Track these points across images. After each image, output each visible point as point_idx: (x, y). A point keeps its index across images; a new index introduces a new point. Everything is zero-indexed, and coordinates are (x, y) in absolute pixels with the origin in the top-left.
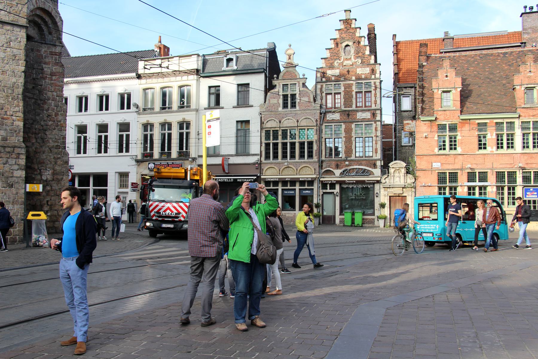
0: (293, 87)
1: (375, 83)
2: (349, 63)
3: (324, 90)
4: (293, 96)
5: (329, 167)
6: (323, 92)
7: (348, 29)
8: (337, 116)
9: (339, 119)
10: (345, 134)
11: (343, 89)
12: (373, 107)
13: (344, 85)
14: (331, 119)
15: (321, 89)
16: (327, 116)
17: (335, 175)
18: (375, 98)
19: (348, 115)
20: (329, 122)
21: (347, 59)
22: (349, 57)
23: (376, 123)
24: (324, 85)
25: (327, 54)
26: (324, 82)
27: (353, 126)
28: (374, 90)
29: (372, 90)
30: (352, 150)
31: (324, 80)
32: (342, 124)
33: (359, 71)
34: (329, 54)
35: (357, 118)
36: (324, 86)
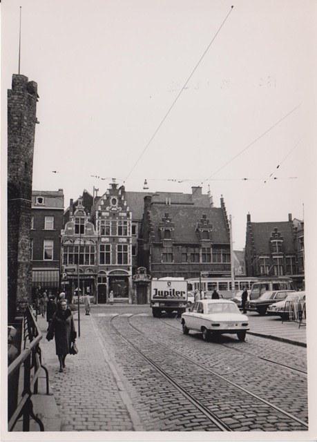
2: (115, 209)
4: (82, 227)
12: (128, 236)
13: (112, 222)
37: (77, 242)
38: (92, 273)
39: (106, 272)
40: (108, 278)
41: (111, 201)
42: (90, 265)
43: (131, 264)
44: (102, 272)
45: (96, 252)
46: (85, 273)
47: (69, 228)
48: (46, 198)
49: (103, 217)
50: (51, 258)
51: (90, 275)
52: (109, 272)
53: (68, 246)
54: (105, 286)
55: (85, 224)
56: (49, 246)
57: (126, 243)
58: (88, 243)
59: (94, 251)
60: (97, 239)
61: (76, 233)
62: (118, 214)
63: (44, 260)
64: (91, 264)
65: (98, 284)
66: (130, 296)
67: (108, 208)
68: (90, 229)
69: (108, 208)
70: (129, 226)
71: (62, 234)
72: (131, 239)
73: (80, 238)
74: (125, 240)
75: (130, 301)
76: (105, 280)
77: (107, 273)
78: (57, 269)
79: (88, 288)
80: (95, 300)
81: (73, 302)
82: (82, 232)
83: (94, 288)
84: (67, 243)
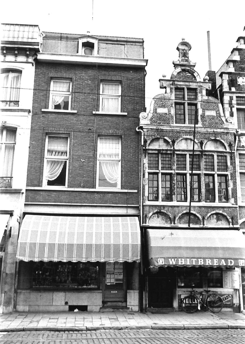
3: (234, 102)
6: (234, 107)
24: (234, 96)
26: (233, 93)
31: (233, 89)
42: (217, 204)
48: (103, 45)
50: (115, 185)
58: (209, 146)
60: (231, 138)
63: (98, 189)
64: (220, 201)
68: (213, 113)
71: (143, 122)
78: (131, 211)
81: (176, 304)
84: (156, 146)
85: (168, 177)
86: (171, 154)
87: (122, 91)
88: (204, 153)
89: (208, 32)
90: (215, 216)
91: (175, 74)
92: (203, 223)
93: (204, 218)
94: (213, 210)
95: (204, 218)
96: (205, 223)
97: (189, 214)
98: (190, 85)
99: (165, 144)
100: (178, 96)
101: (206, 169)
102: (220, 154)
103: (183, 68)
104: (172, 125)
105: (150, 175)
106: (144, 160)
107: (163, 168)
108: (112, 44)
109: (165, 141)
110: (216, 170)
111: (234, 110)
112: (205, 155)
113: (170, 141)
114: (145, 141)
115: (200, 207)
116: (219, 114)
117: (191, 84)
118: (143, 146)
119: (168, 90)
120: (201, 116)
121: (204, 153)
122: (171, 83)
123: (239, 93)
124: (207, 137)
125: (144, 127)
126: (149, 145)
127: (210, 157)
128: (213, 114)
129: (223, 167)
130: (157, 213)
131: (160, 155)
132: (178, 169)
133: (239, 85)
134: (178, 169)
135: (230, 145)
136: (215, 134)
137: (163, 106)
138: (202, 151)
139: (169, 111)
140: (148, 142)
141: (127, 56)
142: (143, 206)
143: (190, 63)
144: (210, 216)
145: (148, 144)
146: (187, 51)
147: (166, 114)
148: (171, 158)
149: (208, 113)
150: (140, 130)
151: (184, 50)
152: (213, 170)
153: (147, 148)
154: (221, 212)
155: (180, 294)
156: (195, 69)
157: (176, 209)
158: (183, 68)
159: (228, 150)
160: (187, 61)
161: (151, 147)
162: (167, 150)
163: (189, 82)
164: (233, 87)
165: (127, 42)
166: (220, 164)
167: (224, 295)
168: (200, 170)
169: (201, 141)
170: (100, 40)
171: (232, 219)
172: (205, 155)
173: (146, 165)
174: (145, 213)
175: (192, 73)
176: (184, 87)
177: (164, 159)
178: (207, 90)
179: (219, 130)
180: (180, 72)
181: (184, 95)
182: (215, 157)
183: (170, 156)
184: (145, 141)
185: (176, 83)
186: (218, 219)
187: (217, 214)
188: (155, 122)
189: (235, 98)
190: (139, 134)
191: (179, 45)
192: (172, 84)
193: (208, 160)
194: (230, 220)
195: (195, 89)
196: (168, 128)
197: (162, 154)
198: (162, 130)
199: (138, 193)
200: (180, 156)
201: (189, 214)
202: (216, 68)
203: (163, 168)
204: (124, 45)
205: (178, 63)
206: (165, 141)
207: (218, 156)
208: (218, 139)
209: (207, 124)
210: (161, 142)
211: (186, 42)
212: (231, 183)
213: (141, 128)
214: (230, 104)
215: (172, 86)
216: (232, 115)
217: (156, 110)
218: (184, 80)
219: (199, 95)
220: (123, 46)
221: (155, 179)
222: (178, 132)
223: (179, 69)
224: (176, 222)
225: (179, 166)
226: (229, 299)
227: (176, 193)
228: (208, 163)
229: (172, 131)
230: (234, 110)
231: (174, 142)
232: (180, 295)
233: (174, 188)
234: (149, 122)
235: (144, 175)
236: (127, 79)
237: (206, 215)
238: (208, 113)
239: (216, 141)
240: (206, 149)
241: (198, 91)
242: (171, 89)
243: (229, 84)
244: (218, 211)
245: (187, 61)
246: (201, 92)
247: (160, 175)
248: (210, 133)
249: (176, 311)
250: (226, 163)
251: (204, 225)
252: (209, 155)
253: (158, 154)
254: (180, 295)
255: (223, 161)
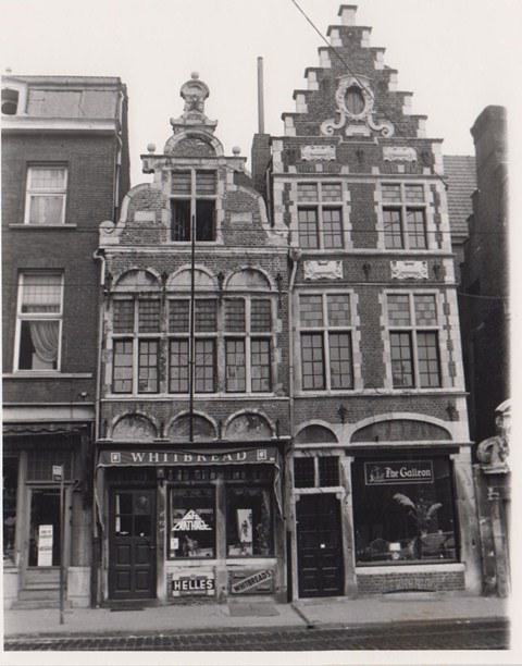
0: (203, 181)
1: (433, 188)
2: (364, 131)
3: (293, 195)
4: (207, 208)
5: (318, 418)
6: (292, 203)
7: (353, 51)
8: (333, 269)
9: (341, 276)
10: (361, 321)
11: (347, 196)
12: (433, 248)
13: (351, 187)
14: (319, 277)
15: (285, 195)
16: (306, 268)
17: (337, 441)
18: (438, 227)
19: (366, 269)
20: (310, 283)
21: (354, 122)
22: (361, 116)
23: (445, 293)
24: (294, 182)
25: (300, 107)
27: (382, 298)
28: (432, 204)
29: (427, 204)
30: (384, 365)
31: (292, 170)
32: (351, 291)
33: (389, 152)
34: (305, 106)
35: (393, 276)
36: (294, 186)
37: (179, 282)
38: (260, 435)
39: (337, 429)
40: (346, 463)
41: (339, 95)
43: (459, 385)
44: (314, 432)
45: (278, 326)
46: (229, 436)
47: (142, 217)
48: (37, 94)
49: (306, 168)
51: (253, 446)
52: (350, 429)
53: (135, 297)
54: (333, 499)
55: (219, 197)
56: (44, 308)
57: (424, 283)
58: (237, 282)
59: (269, 327)
60: (282, 266)
61: (175, 238)
62: (378, 150)
65: (297, 491)
66: (467, 553)
67: (326, 128)
68: (247, 218)
69: (326, 128)
70: (436, 203)
71: (104, 240)
72: (449, 265)
73: (193, 258)
74: (420, 269)
75: (472, 580)
76: (331, 474)
77: (344, 434)
79: (244, 515)
80: (281, 582)
81: (162, 591)
82: (207, 232)
83: (277, 520)
85: (153, 346)
86: (159, 300)
87: (69, 182)
88: (224, 297)
89: (260, 59)
90: (244, 419)
91: (173, 144)
92: (220, 434)
93: (220, 424)
94: (240, 408)
95: (220, 424)
96: (223, 435)
97: (191, 416)
98: (201, 165)
99: (148, 282)
100: (179, 187)
101: (229, 328)
102: (258, 298)
103: (189, 131)
104: (163, 243)
105: (142, 344)
106: (106, 314)
107: (142, 329)
108: (58, 91)
109: (149, 275)
110: (248, 328)
111: (293, 209)
112: (227, 300)
113: (157, 275)
114: (109, 278)
115: (214, 402)
116: (259, 218)
117: (203, 161)
118: (104, 287)
119: (158, 174)
120: (222, 223)
121: (224, 297)
122: (164, 161)
123: (304, 176)
124: (231, 262)
125: (106, 251)
126: (117, 284)
127: (238, 304)
128: (246, 220)
129: (263, 323)
130: (129, 416)
131: (137, 304)
132: (172, 328)
133: (305, 160)
134: (172, 328)
135: (278, 279)
136: (250, 258)
137: (147, 208)
138: (220, 293)
139: (158, 216)
140: (115, 278)
141: (84, 114)
142: (101, 403)
143: (204, 121)
144: (233, 419)
145: (113, 283)
146: (201, 100)
147: (152, 222)
148: (159, 307)
149: (235, 219)
150: (101, 257)
151: (195, 96)
152: (243, 329)
153: (112, 290)
154: (255, 411)
155: (170, 572)
156: (215, 134)
157: (167, 408)
158: (189, 131)
159: (274, 289)
160: (198, 117)
161: (119, 289)
162: (150, 293)
163: (201, 158)
164: (291, 164)
165: (85, 85)
166: (258, 317)
167: (257, 571)
168: (216, 331)
169: (221, 273)
170: (30, 84)
171: (277, 423)
172: (227, 300)
173: (110, 324)
174: (105, 416)
175: (208, 140)
176: (190, 168)
177: (147, 311)
178: (236, 172)
179: (257, 251)
180: (184, 140)
181: (190, 184)
182: (248, 304)
183: (157, 304)
184: (109, 278)
185: (174, 161)
186: (251, 426)
187: (248, 415)
188: (129, 239)
189: (294, 186)
190: (98, 263)
191: (183, 87)
192: (166, 164)
193: (232, 310)
194: (273, 426)
195: (213, 172)
196: (156, 251)
197: (141, 301)
198: (143, 255)
199: (94, 378)
200: (176, 304)
201: (191, 416)
202: (276, 128)
203: (142, 329)
204: (81, 91)
205: (180, 123)
206: (149, 275)
207: (252, 301)
208: (255, 267)
209: (234, 238)
210: (141, 276)
211: (200, 83)
212: (277, 354)
213: (102, 252)
214: (287, 202)
215: (165, 168)
216: (287, 221)
217: (133, 215)
218: (192, 155)
219: (220, 184)
220: (78, 94)
221: (240, 349)
222: (174, 257)
223: (182, 134)
224: (165, 434)
225: (175, 323)
226: (268, 578)
227: (167, 377)
228: (233, 317)
229: (162, 256)
230: (293, 209)
231: (165, 277)
232: (172, 574)
233: (164, 367)
234: (116, 240)
235: (104, 343)
236: (80, 159)
237: (226, 417)
238: (235, 219)
239: (250, 271)
240: (229, 289)
241: (219, 175)
242: (164, 172)
243: (283, 160)
244: (249, 410)
245: (198, 117)
246: (224, 177)
247: (248, 340)
248: (238, 257)
249: (161, 605)
250: (270, 314)
251: (220, 437)
252: (235, 300)
253: (132, 301)
254: (172, 574)
255: (263, 310)
